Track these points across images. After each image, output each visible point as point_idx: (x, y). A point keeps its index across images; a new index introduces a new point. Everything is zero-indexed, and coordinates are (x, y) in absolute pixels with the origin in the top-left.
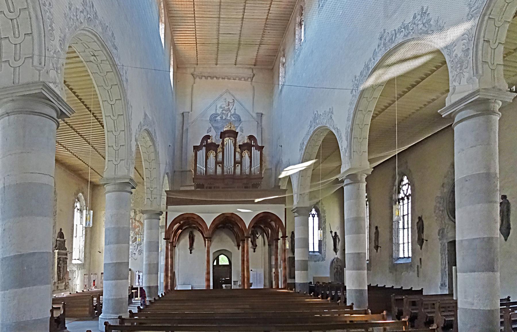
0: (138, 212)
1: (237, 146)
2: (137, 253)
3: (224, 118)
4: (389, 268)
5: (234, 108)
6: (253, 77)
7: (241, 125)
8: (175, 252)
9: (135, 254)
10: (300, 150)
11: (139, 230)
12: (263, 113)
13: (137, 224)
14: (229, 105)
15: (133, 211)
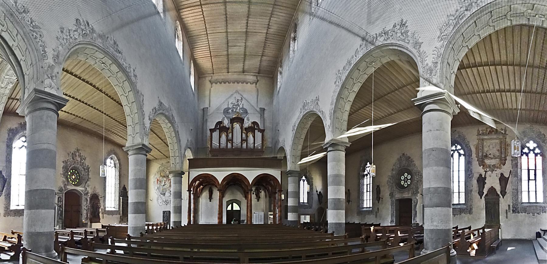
1: (244, 129)
3: (234, 111)
4: (357, 213)
5: (242, 104)
6: (257, 82)
7: (247, 116)
8: (199, 201)
10: (292, 131)
12: (265, 108)
14: (238, 101)
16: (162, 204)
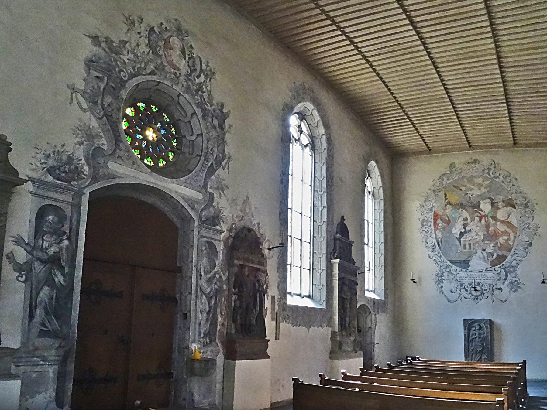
0: (500, 205)
2: (506, 288)
9: (500, 289)
11: (509, 239)
13: (501, 227)
15: (489, 201)
16: (456, 296)
